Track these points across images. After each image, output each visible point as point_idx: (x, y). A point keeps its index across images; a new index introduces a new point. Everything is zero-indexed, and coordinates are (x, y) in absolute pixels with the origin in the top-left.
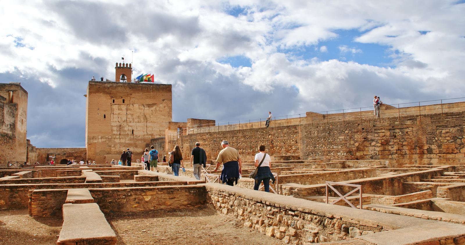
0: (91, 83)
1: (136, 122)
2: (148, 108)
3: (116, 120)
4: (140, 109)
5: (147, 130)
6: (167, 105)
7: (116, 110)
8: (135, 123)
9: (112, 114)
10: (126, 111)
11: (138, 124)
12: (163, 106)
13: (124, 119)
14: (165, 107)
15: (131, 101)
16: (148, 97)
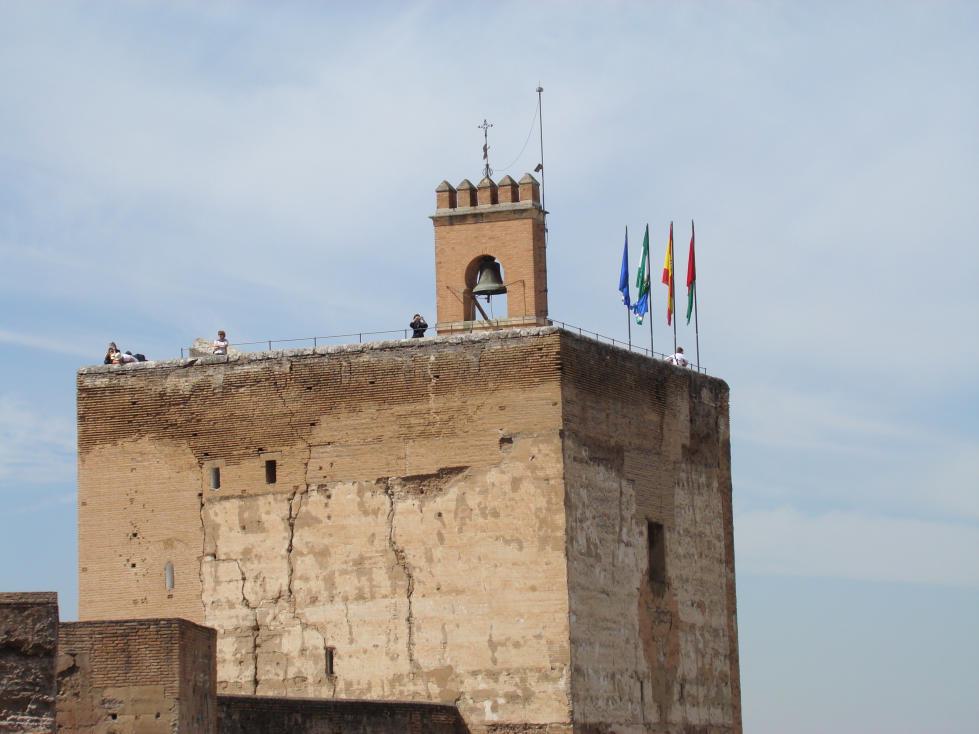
0: (88, 382)
1: (346, 599)
2: (417, 503)
3: (230, 591)
4: (366, 513)
5: (410, 644)
6: (533, 469)
7: (231, 529)
8: (339, 605)
9: (209, 558)
10: (287, 534)
11: (353, 607)
12: (506, 478)
13: (278, 582)
14: (516, 483)
15: (313, 466)
16: (410, 427)
